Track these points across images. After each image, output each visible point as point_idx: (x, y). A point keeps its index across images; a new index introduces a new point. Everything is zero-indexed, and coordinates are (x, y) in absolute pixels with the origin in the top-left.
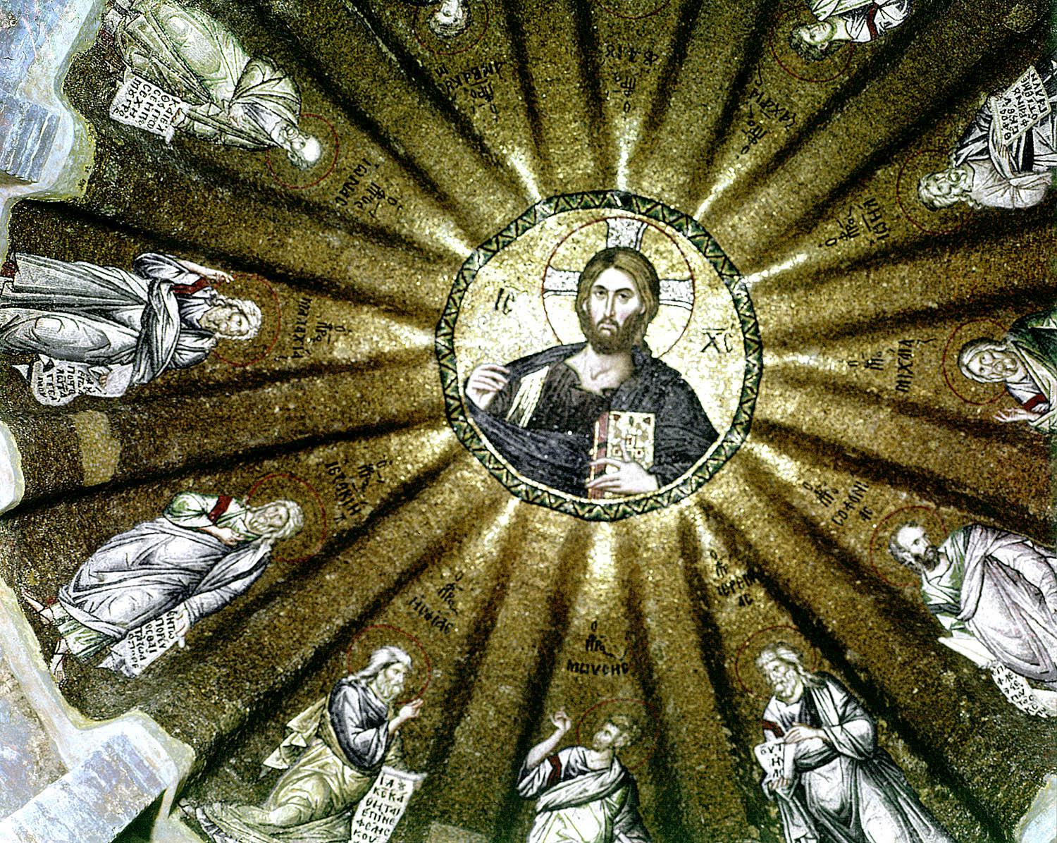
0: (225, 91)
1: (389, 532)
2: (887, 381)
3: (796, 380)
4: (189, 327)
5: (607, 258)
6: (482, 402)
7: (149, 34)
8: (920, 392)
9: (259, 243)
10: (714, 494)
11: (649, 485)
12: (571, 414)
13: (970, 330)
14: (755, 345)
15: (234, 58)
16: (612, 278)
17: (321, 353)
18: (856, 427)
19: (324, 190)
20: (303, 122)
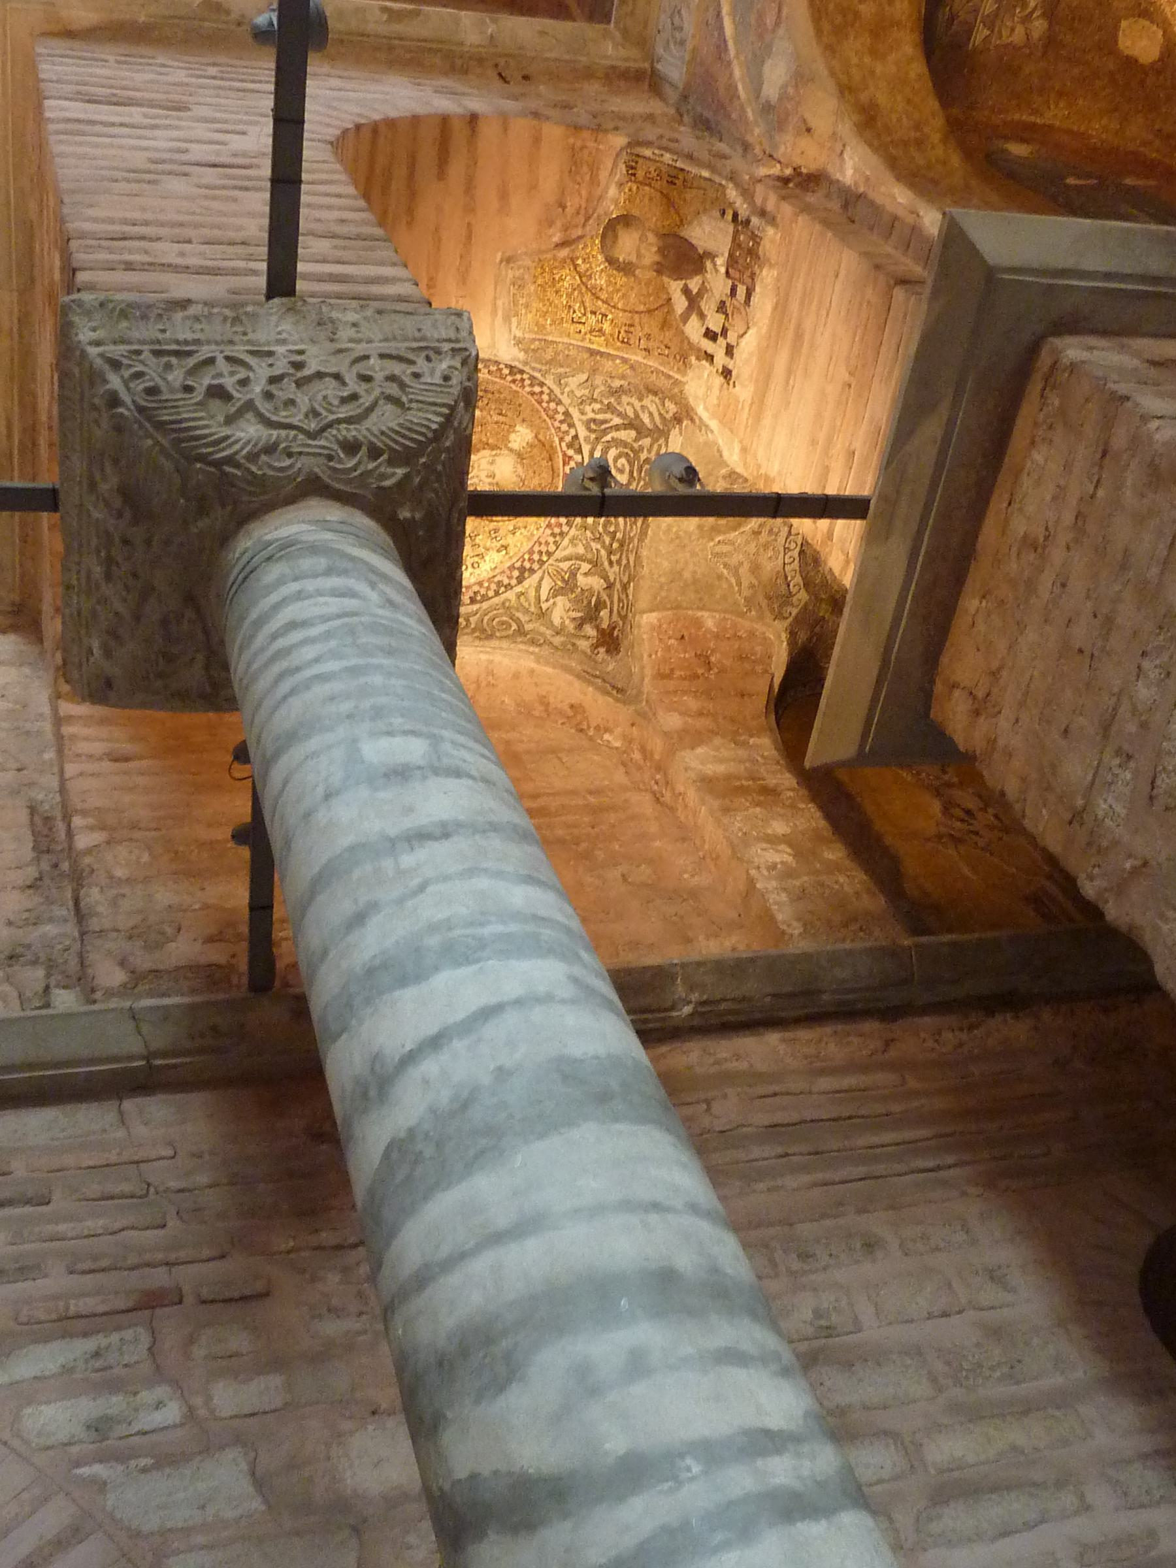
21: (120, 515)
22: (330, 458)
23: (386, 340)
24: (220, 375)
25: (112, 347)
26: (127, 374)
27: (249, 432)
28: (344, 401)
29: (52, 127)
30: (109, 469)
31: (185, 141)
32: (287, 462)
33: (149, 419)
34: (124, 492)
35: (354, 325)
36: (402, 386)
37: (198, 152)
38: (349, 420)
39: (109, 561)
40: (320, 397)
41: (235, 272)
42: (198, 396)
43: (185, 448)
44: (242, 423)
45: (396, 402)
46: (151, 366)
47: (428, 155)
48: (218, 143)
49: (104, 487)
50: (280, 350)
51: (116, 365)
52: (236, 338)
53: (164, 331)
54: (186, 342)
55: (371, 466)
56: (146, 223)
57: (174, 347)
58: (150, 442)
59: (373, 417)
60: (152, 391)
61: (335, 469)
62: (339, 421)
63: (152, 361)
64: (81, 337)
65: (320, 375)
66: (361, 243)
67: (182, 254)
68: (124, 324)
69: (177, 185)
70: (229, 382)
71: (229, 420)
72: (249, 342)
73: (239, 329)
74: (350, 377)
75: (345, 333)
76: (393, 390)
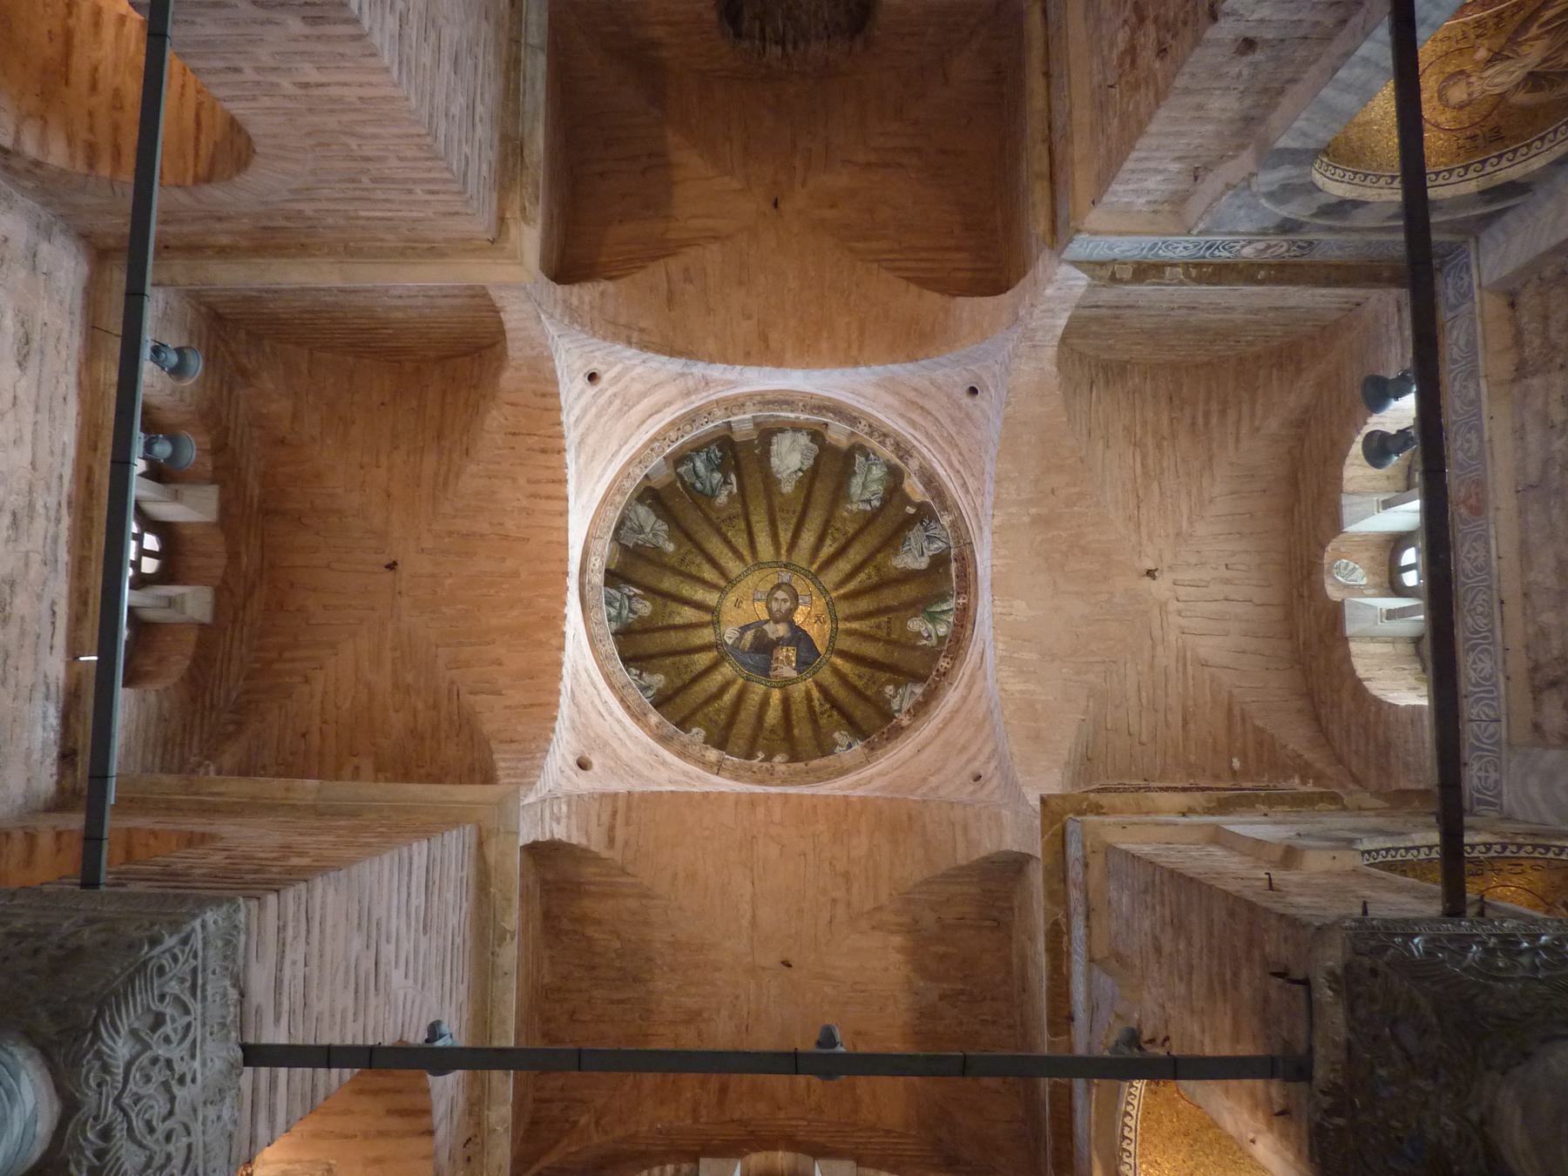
0: (648, 530)
1: (697, 688)
2: (882, 633)
3: (850, 633)
4: (631, 610)
5: (778, 587)
6: (730, 642)
7: (632, 515)
8: (894, 636)
9: (650, 580)
10: (819, 676)
11: (794, 674)
12: (765, 647)
13: (910, 613)
14: (835, 620)
15: (653, 518)
16: (780, 594)
17: (671, 622)
18: (870, 650)
19: (674, 561)
20: (670, 539)
21: (61, 947)
22: (96, 1118)
23: (205, 1146)
24: (173, 1020)
25: (200, 936)
26: (177, 951)
27: (122, 1049)
28: (149, 1123)
29: (405, 850)
30: (100, 937)
31: (397, 941)
32: (93, 1084)
33: (138, 971)
34: (79, 949)
35: (219, 1118)
36: (162, 1168)
37: (388, 951)
38: (130, 1129)
39: (21, 936)
40: (153, 1102)
41: (278, 1005)
42: (156, 1006)
43: (109, 1001)
44: (130, 1043)
45: (147, 1166)
46: (183, 968)
47: (404, 1101)
48: (396, 962)
49: (86, 933)
50: (197, 1064)
51: (185, 941)
52: (208, 1028)
53: (214, 973)
54: (204, 990)
55: (89, 1153)
56: (322, 932)
57: (200, 981)
58: (117, 971)
59: (134, 1148)
60: (161, 971)
61: (85, 1123)
62: (129, 1122)
63: (187, 968)
64: (209, 914)
65: (172, 1099)
66: (308, 1088)
67: (294, 963)
68: (220, 943)
69: (357, 943)
70: (168, 1028)
71: (134, 1033)
72: (203, 1040)
73: (216, 1029)
74: (169, 1124)
75: (211, 1112)
76: (159, 1160)
